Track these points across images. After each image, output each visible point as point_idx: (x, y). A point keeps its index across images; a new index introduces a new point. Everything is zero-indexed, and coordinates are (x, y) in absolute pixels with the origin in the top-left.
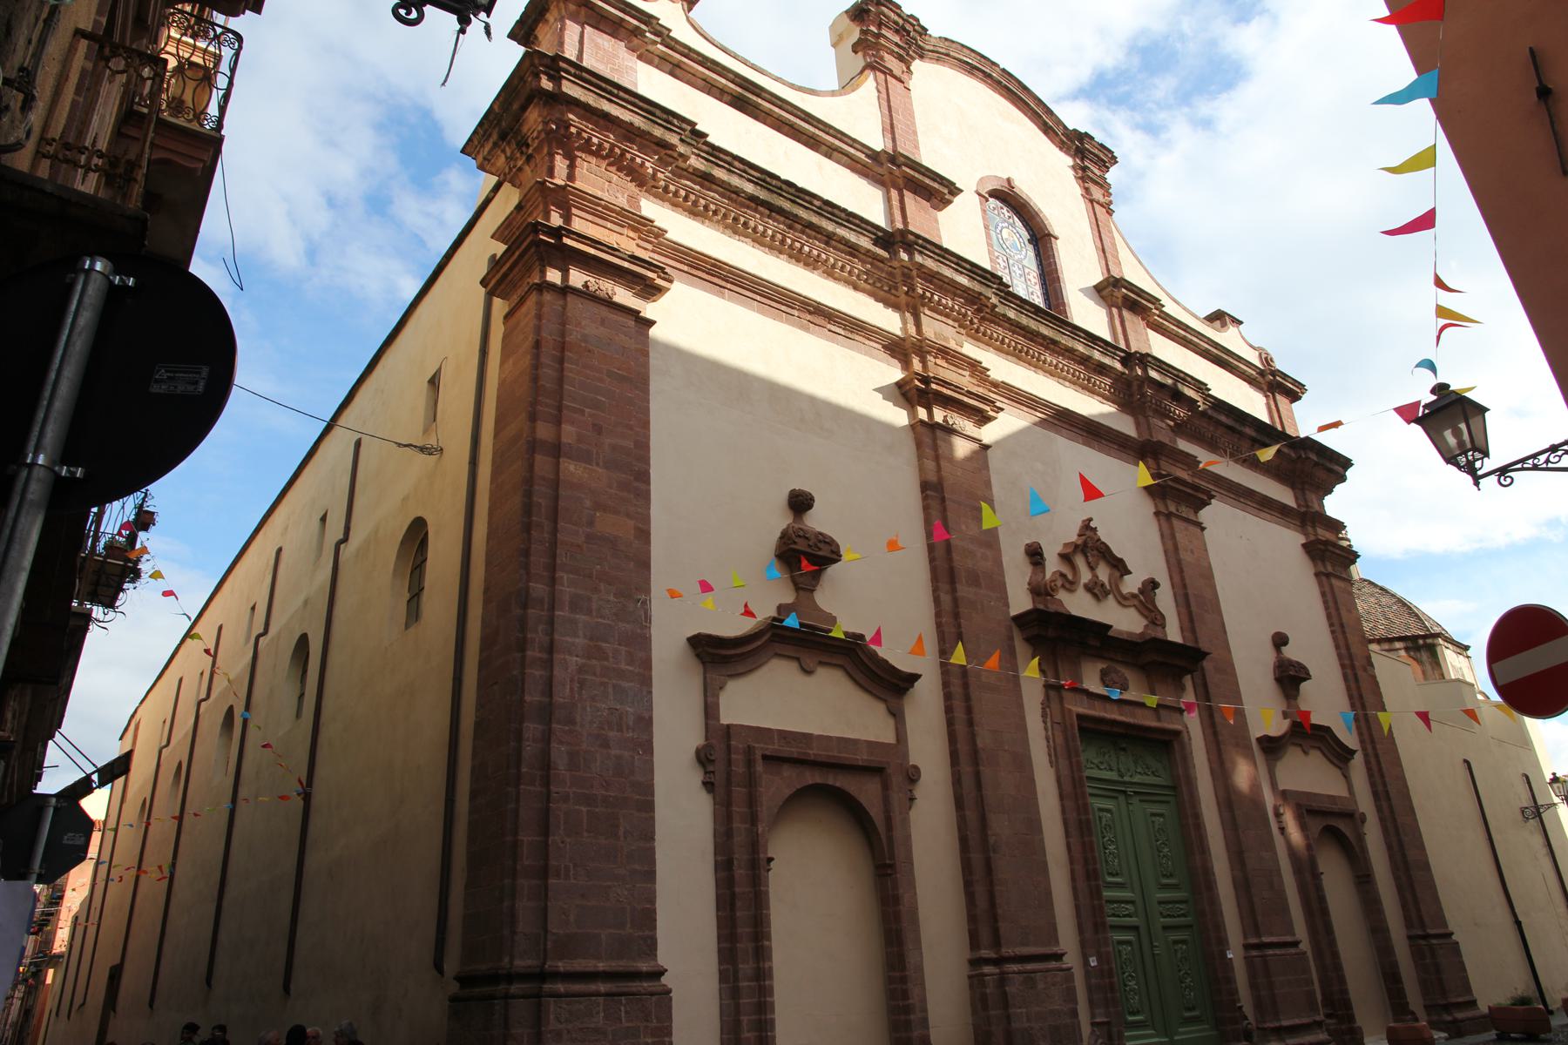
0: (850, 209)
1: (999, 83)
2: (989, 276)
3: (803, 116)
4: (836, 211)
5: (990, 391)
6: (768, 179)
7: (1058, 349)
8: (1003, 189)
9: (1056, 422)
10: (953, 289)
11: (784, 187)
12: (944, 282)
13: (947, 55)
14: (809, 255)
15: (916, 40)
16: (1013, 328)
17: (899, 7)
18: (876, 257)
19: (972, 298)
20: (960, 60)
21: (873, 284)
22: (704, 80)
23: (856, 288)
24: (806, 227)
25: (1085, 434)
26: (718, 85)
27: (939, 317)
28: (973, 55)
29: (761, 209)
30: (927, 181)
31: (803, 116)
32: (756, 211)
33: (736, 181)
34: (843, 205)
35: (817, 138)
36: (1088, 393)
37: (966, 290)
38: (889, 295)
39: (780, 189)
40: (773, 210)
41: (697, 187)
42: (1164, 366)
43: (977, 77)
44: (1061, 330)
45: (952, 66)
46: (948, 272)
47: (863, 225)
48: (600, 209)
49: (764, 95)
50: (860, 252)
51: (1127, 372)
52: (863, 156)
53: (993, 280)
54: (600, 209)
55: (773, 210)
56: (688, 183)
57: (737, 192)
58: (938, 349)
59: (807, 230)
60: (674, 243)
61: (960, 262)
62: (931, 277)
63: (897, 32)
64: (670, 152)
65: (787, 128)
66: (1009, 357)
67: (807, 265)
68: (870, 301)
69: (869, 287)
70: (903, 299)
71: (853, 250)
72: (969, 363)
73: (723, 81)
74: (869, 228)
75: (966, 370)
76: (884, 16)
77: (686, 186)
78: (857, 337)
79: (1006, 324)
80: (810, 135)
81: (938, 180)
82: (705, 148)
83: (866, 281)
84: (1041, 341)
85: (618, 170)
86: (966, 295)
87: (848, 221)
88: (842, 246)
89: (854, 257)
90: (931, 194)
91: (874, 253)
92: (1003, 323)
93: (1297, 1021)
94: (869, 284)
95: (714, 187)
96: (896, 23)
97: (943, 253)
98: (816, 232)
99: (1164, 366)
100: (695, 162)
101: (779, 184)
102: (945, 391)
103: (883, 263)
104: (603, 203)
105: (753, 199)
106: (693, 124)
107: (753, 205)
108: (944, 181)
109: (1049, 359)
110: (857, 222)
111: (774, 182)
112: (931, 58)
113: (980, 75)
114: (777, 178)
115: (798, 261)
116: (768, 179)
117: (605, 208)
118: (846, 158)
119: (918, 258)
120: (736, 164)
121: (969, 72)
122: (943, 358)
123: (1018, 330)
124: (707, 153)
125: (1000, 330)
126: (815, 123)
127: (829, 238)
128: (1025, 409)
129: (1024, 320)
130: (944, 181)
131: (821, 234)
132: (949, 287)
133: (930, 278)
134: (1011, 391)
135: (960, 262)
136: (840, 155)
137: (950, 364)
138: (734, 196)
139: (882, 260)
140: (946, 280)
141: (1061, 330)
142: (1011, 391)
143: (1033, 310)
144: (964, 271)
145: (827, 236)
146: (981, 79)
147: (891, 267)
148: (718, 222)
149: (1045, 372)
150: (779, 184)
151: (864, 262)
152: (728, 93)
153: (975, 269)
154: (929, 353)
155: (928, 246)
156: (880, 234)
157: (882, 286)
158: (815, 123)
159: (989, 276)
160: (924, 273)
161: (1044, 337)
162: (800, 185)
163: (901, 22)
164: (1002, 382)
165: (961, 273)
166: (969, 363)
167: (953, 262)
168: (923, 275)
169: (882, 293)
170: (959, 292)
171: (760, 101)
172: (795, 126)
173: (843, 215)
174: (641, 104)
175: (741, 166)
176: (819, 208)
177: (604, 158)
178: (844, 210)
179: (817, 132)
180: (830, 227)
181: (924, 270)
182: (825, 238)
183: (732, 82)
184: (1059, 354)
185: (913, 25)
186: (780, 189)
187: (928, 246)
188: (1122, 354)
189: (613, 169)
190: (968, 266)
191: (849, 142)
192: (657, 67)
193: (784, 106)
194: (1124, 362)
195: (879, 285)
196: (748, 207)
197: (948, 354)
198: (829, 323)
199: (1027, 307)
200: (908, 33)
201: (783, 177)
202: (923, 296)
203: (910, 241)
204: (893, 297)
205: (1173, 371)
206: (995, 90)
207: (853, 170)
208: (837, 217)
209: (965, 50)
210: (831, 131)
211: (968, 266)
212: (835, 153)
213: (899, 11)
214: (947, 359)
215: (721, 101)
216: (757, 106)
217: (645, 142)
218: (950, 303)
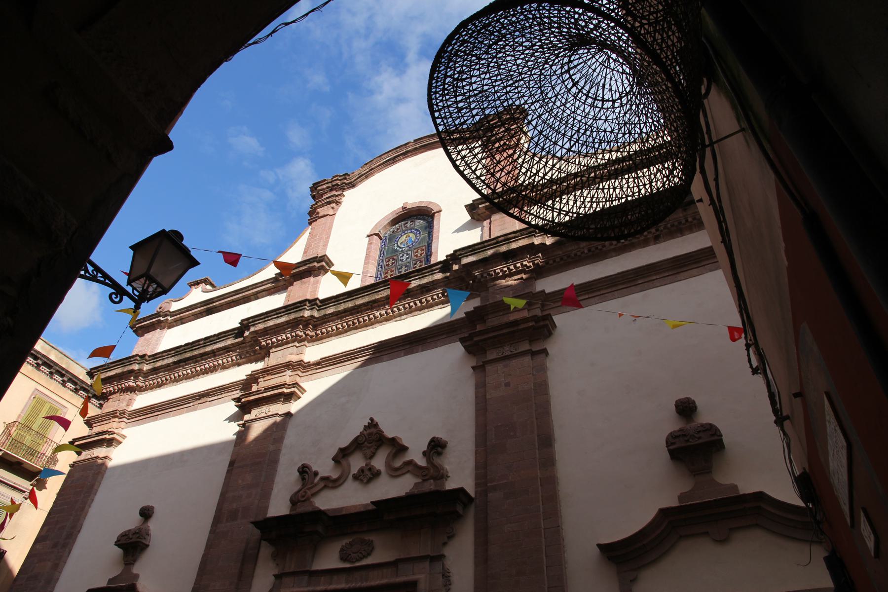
0: (217, 333)
1: (416, 149)
2: (299, 305)
3: (234, 293)
4: (211, 339)
5: (316, 369)
6: (178, 350)
7: (382, 303)
8: (399, 214)
9: (377, 355)
10: (281, 328)
11: (185, 347)
12: (274, 329)
13: (372, 169)
14: (210, 367)
15: (344, 183)
16: (339, 316)
17: (325, 180)
18: (238, 344)
19: (293, 324)
20: (383, 163)
21: (246, 357)
22: (193, 315)
23: (239, 365)
25: (408, 346)
26: (197, 313)
27: (283, 348)
28: (390, 153)
29: (181, 364)
30: (301, 269)
31: (234, 293)
32: (180, 367)
33: (166, 362)
34: (212, 334)
35: (246, 296)
36: (427, 310)
37: (287, 323)
38: (256, 356)
39: (185, 349)
40: (186, 361)
41: (155, 376)
42: (476, 247)
43: (401, 160)
44: (376, 290)
45: (379, 171)
46: (271, 323)
47: (227, 334)
48: (101, 418)
49: (214, 300)
50: (231, 348)
51: (448, 274)
52: (269, 285)
53: (302, 304)
54: (101, 418)
55: (186, 361)
56: (151, 377)
57: (168, 365)
58: (262, 372)
59: (203, 357)
60: (134, 410)
61: (277, 312)
62: (266, 332)
63: (331, 190)
64: (136, 372)
65: (232, 304)
66: (348, 333)
67: (212, 372)
68: (249, 365)
69: (244, 360)
70: (263, 352)
71: (227, 350)
72: (284, 366)
73: (198, 310)
74: (230, 333)
75: (286, 371)
76: (321, 190)
77: (151, 378)
78: (223, 395)
79: (334, 317)
80: (242, 298)
81: (307, 263)
82: (151, 358)
83: (241, 358)
84: (365, 307)
85: (124, 393)
86: (290, 325)
90: (310, 271)
91: (237, 342)
92: (331, 318)
94: (244, 358)
95: (160, 370)
96: (328, 188)
97: (266, 315)
98: (208, 355)
99: (476, 247)
100: (146, 367)
101: (183, 348)
102: (251, 398)
103: (243, 343)
104: (100, 416)
105: (174, 363)
106: (137, 355)
107: (177, 365)
108: (311, 261)
109: (377, 314)
110: (223, 335)
111: (181, 349)
112: (360, 181)
113: (401, 157)
114: (181, 346)
115: (207, 373)
116: (178, 350)
117: (102, 417)
118: (264, 293)
119: (252, 329)
120: (164, 354)
121: (393, 163)
122: (268, 375)
123: (343, 314)
124: (153, 359)
125: (331, 324)
126: (241, 291)
127: (214, 353)
128: (347, 363)
129: (342, 307)
130: (311, 261)
131: (210, 354)
132: (278, 329)
133: (265, 333)
134: (331, 360)
135: (277, 312)
136: (260, 294)
137: (274, 374)
138: (169, 368)
139: (242, 343)
140: (273, 327)
141: (376, 290)
142: (331, 360)
143: (346, 296)
144: (282, 314)
145: (213, 353)
146: (403, 158)
147: (249, 342)
148: (170, 382)
149: (381, 322)
150: (183, 348)
151: (235, 351)
152: (203, 312)
153: (289, 308)
154: (259, 378)
155: (256, 319)
156: (236, 331)
157: (250, 354)
158: (241, 291)
159: (299, 305)
160: (261, 333)
161: (363, 304)
162: (191, 341)
163: (330, 185)
164: (321, 359)
165: (281, 316)
166: (284, 366)
167: (274, 315)
168: (261, 335)
169: (252, 357)
170: (286, 327)
171: (214, 304)
172: (235, 300)
173: (215, 338)
174: (119, 363)
175: (166, 354)
176: (204, 343)
177: (117, 392)
178: (215, 335)
179: (244, 294)
180: (209, 349)
181: (259, 332)
182: (212, 355)
183: (202, 307)
184: (384, 305)
185: (337, 180)
186: (185, 349)
187: (256, 319)
188: (439, 266)
189: (122, 394)
190: (283, 310)
191: (260, 285)
192: (177, 326)
193: (225, 296)
194: (442, 270)
195: (247, 355)
196: (176, 368)
197: (269, 370)
198: (209, 398)
199: (342, 298)
200: (337, 185)
201: (183, 344)
202: (268, 344)
203: (246, 324)
204: (259, 355)
205: (489, 243)
206: (416, 154)
207: (270, 294)
208: (213, 341)
209: (383, 157)
210: (250, 288)
211: (283, 310)
212: (258, 295)
213: (326, 182)
214: (270, 374)
215: (203, 317)
216: (215, 307)
217: (126, 376)
218: (284, 337)
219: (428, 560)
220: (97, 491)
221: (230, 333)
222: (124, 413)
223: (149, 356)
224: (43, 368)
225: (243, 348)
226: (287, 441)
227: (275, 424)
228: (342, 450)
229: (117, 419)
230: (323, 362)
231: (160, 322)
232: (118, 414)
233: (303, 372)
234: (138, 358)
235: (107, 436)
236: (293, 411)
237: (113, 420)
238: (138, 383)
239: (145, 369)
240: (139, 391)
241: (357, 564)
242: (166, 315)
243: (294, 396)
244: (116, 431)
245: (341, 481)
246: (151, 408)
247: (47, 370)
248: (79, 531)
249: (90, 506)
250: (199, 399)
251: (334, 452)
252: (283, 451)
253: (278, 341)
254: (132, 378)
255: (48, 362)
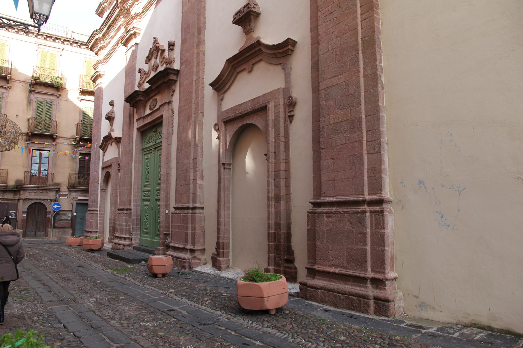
4: (112, 12)
5: (144, 15)
24: (113, 22)
71: (118, 15)
75: (133, 21)
87: (114, 11)
88: (118, 18)
89: (120, 17)
93: (177, 245)
100: (100, 35)
103: (122, 10)
105: (108, 29)
116: (105, 23)
142: (145, 8)
173: (113, 11)
197: (128, 23)
219: (167, 104)
220: (102, 98)
221: (116, 6)
222: (101, 61)
223: (99, 30)
224: (82, 46)
225: (123, 12)
226: (138, 58)
227: (133, 51)
228: (147, 57)
229: (100, 64)
230: (144, 10)
231: (104, 8)
232: (99, 62)
233: (140, 19)
234: (95, 32)
235: (98, 74)
236: (138, 42)
237: (99, 65)
238: (102, 44)
239: (101, 37)
240: (105, 48)
241: (153, 110)
242: (104, 3)
243: (136, 33)
244: (99, 71)
245: (149, 73)
246: (107, 55)
247: (85, 47)
248: (101, 116)
249: (102, 105)
250: (118, 45)
251: (144, 59)
252: (137, 63)
253: (130, 4)
254: (99, 42)
255: (82, 43)
